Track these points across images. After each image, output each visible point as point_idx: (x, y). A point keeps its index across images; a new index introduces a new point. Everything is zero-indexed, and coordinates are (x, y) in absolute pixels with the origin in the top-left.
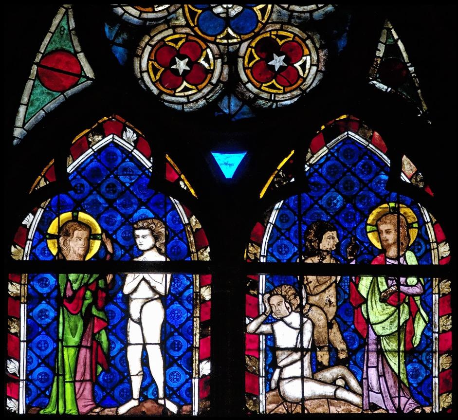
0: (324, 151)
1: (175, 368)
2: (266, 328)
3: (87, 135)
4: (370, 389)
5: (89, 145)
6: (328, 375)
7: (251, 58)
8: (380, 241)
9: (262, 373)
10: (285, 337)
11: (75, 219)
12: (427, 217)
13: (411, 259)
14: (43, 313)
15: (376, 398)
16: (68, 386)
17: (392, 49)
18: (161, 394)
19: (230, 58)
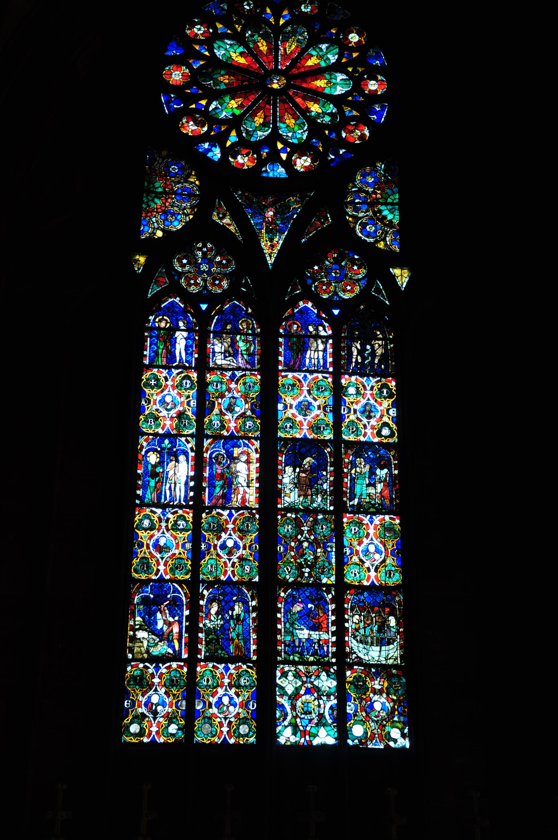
0: (228, 305)
1: (188, 355)
2: (212, 347)
3: (167, 298)
4: (239, 363)
5: (167, 301)
6: (228, 359)
7: (210, 281)
8: (242, 327)
9: (211, 357)
10: (217, 349)
11: (163, 318)
12: (254, 322)
13: (250, 332)
14: (154, 340)
15: (240, 365)
16: (160, 359)
17: (246, 281)
18: (184, 361)
19: (205, 280)
